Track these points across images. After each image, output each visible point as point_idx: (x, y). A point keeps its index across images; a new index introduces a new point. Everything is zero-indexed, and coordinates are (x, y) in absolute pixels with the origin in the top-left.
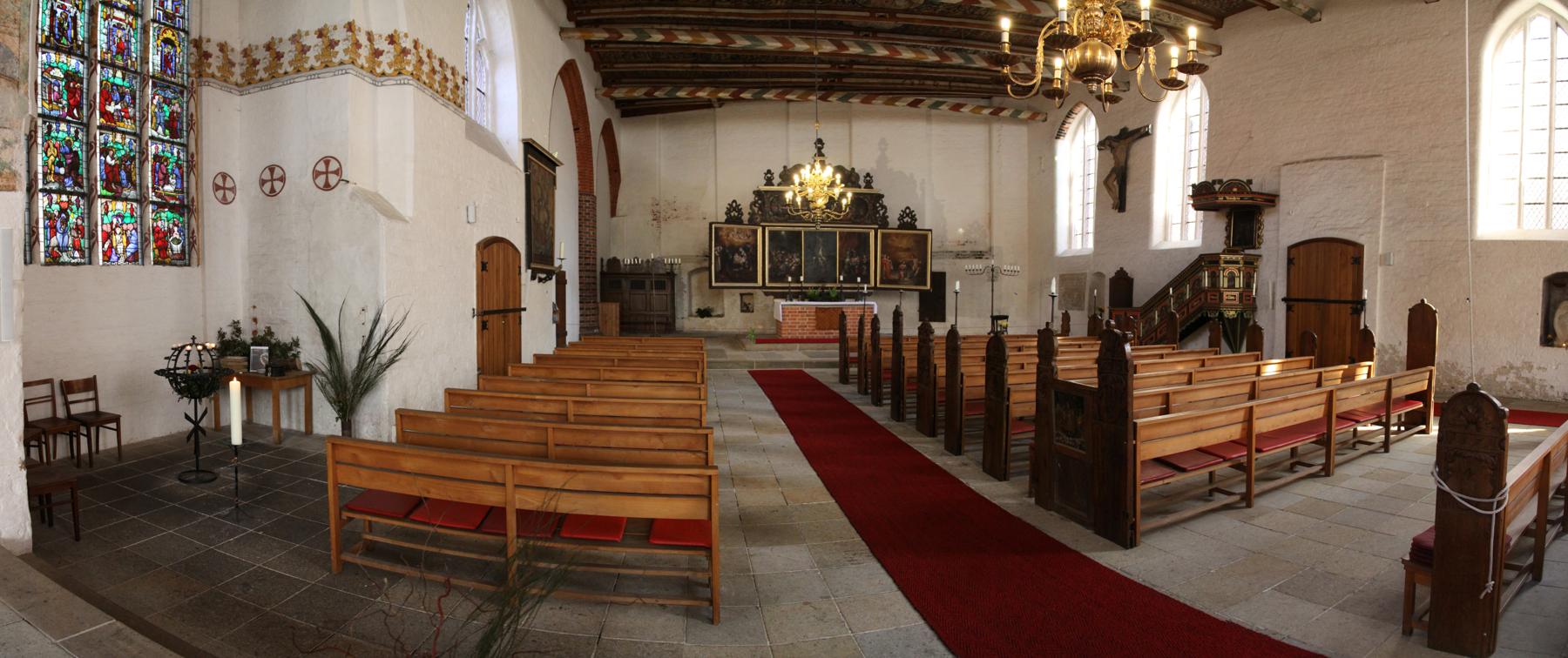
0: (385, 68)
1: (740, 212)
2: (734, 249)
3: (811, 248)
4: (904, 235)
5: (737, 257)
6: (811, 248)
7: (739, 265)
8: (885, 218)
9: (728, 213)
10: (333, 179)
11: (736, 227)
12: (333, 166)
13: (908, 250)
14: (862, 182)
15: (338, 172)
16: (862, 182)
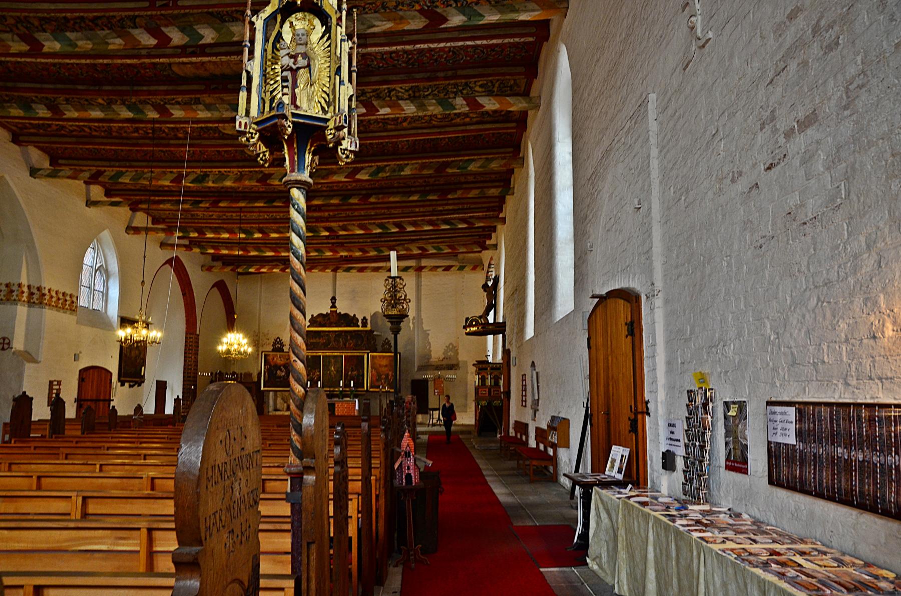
0: (35, 300)
1: (282, 345)
2: (277, 367)
3: (326, 367)
4: (384, 357)
5: (279, 372)
6: (326, 367)
7: (280, 377)
8: (375, 345)
9: (274, 345)
10: (6, 346)
11: (278, 354)
12: (7, 341)
13: (386, 366)
14: (360, 323)
15: (9, 344)
16: (360, 323)
